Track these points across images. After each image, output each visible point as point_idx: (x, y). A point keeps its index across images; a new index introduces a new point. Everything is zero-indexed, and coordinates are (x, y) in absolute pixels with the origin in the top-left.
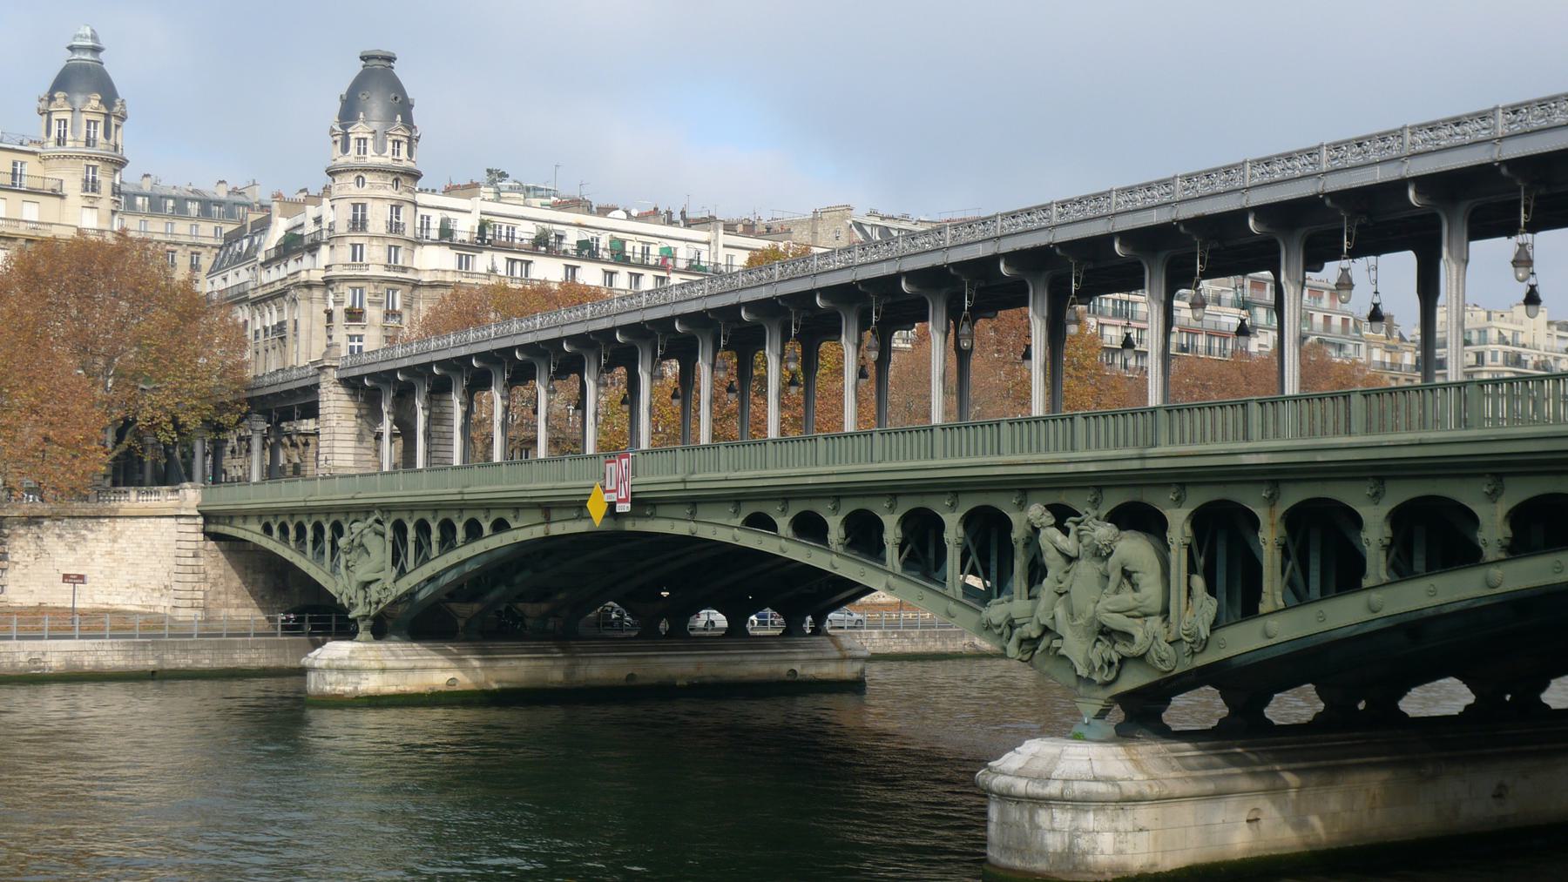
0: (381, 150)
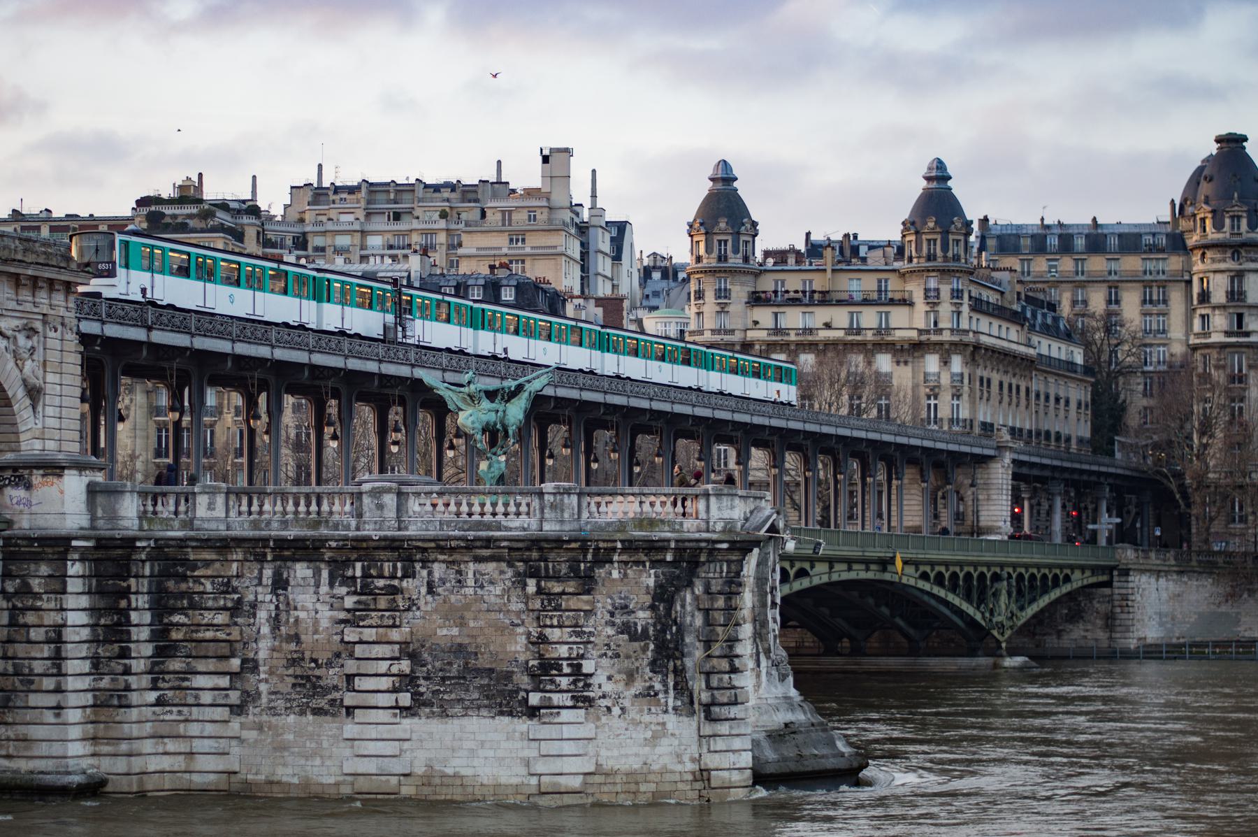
0: (1218, 226)
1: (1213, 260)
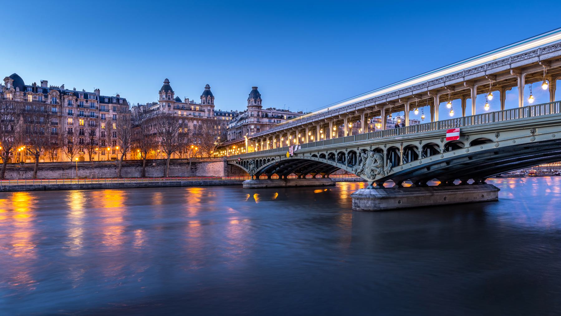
0: (255, 103)
1: (254, 109)
